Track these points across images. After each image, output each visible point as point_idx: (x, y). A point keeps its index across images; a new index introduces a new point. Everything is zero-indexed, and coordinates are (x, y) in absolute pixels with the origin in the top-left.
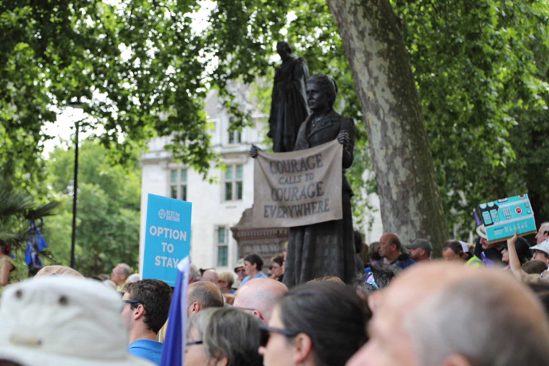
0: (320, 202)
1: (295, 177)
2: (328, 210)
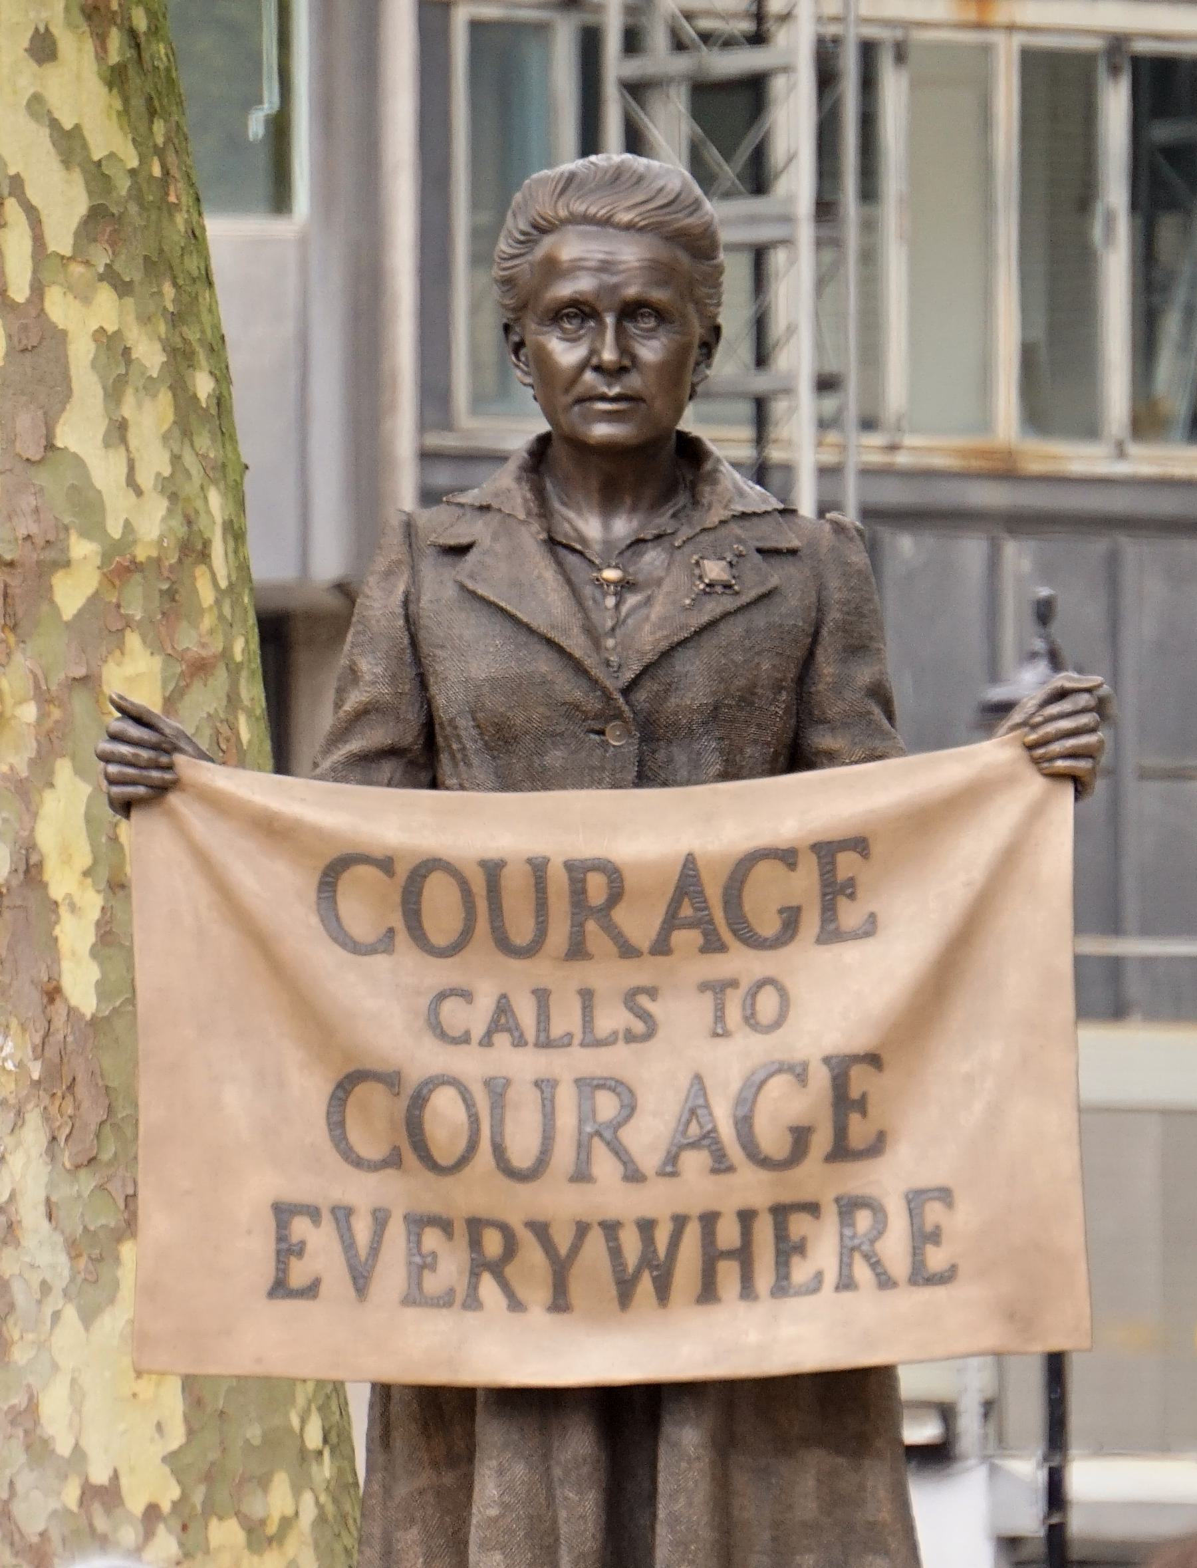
0: (849, 1207)
1: (587, 996)
2: (946, 1277)
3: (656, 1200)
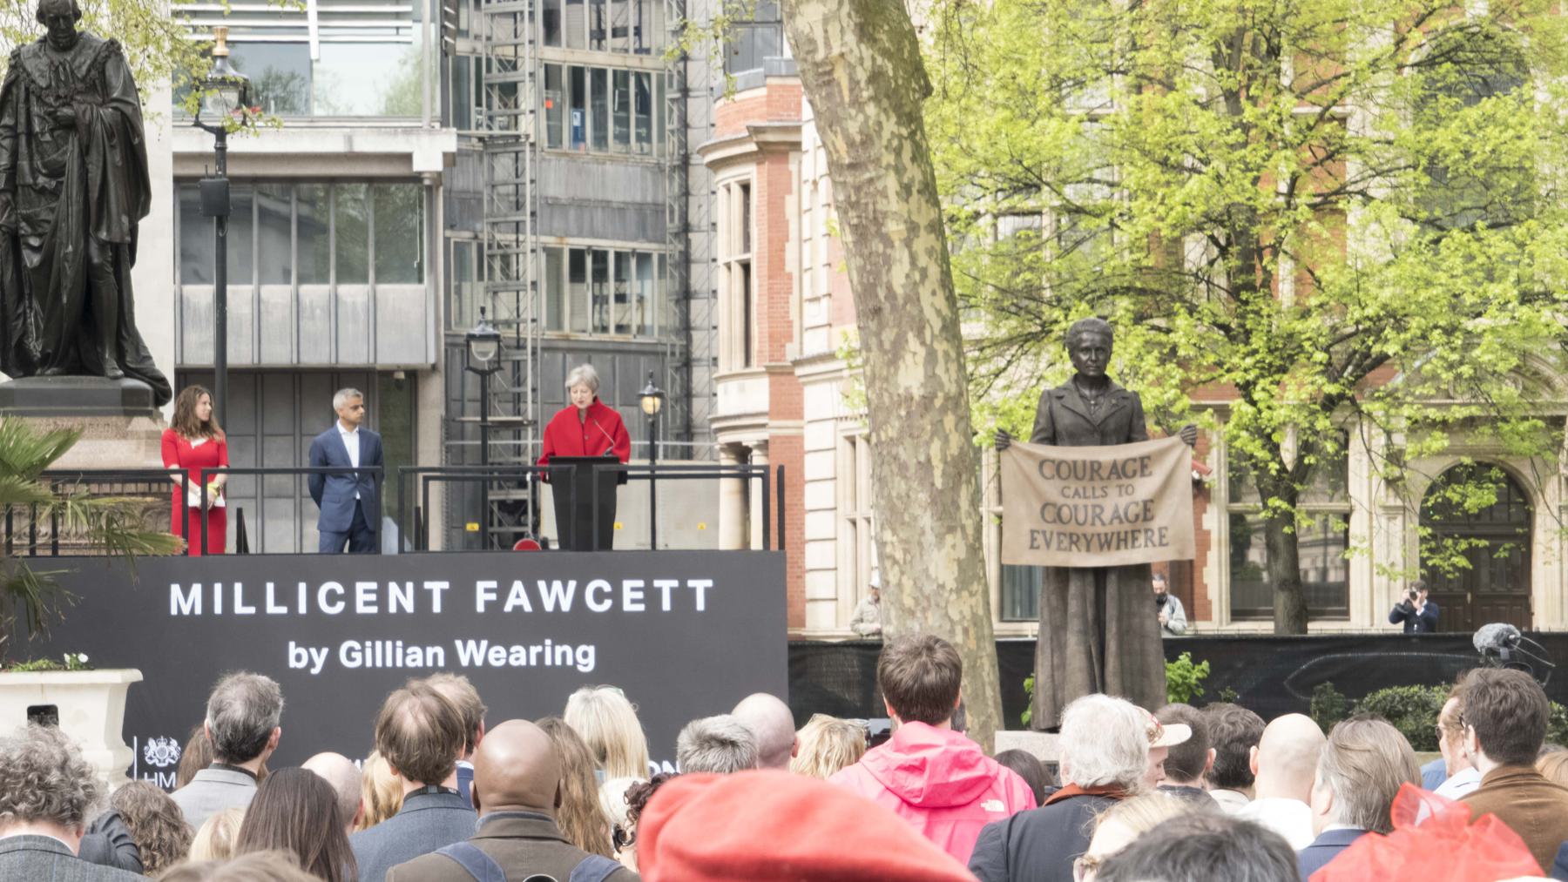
3: (1108, 529)
